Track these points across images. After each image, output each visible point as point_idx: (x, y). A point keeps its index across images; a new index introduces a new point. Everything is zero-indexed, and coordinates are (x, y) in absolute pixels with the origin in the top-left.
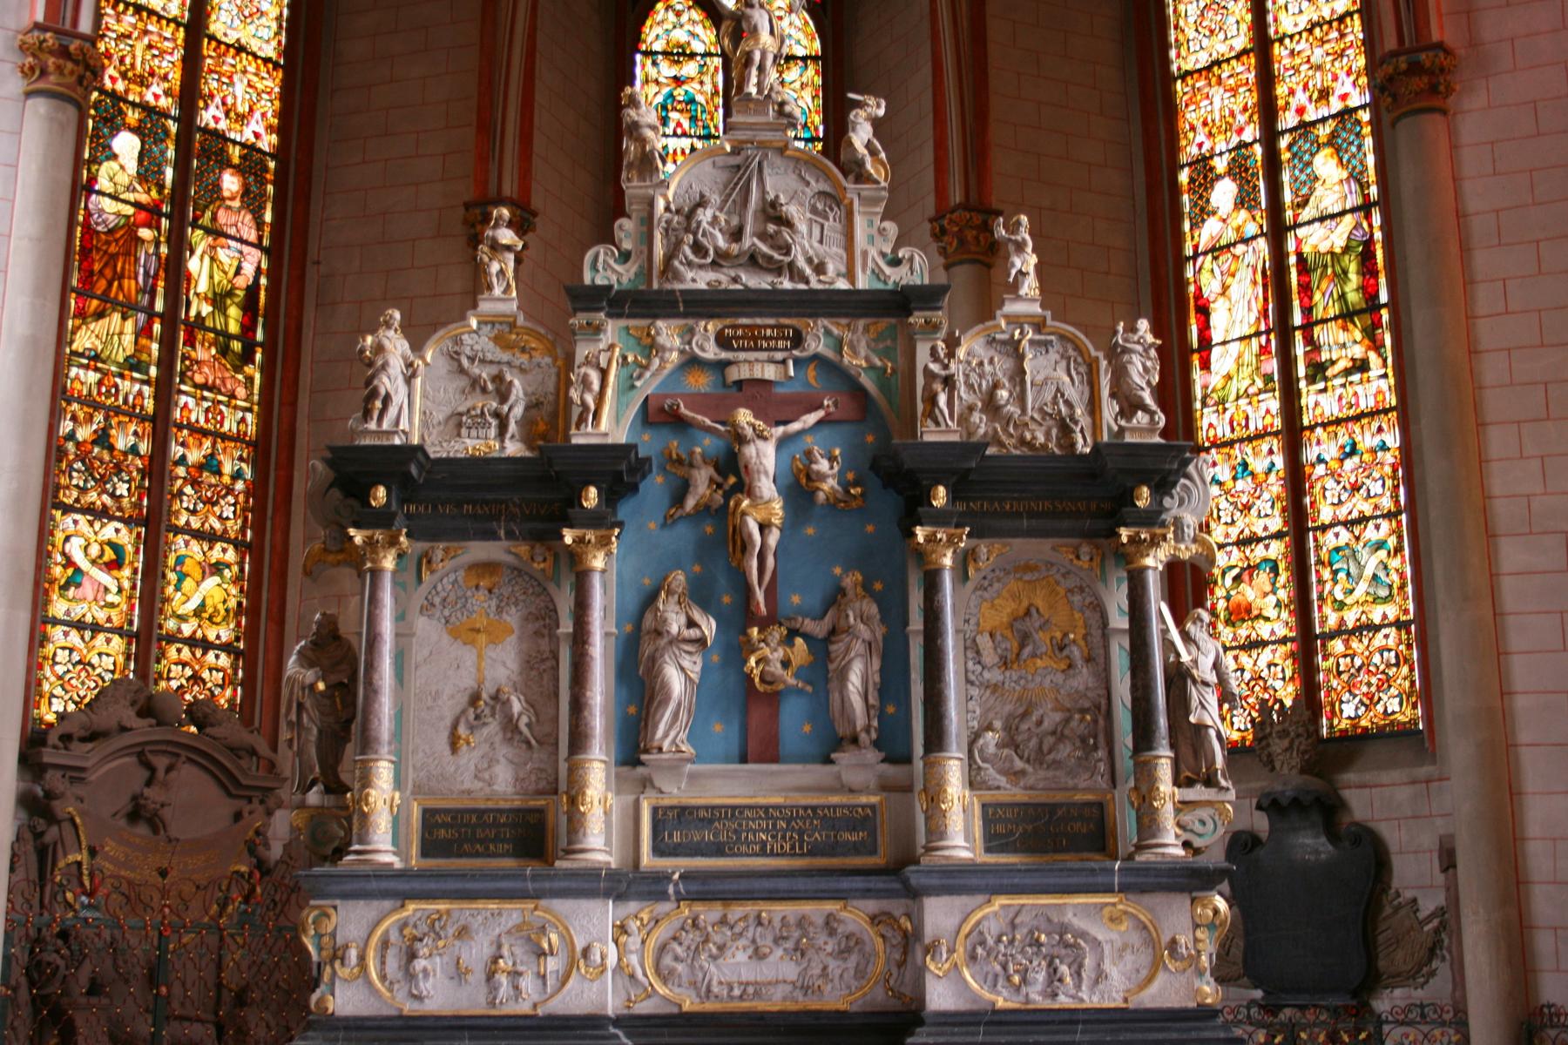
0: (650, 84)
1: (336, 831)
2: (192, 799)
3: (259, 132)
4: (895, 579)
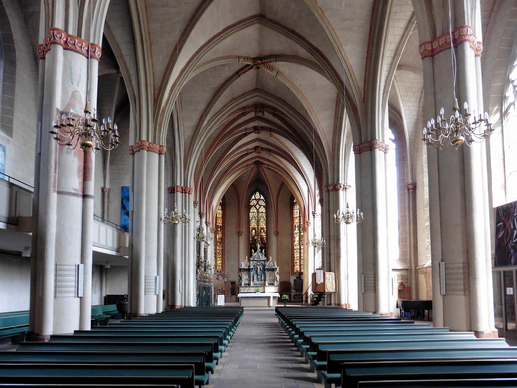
0: (251, 215)
1: (241, 285)
2: (220, 277)
3: (221, 225)
4: (264, 274)
